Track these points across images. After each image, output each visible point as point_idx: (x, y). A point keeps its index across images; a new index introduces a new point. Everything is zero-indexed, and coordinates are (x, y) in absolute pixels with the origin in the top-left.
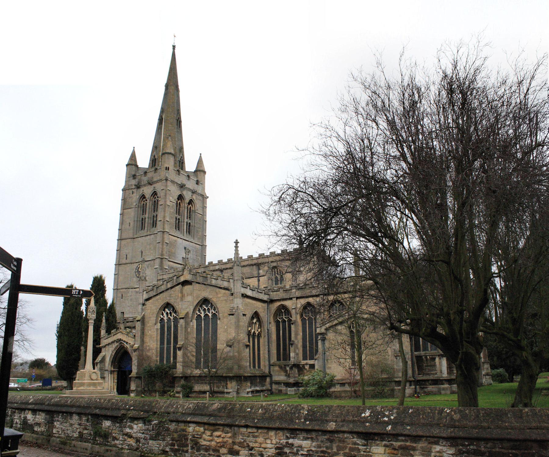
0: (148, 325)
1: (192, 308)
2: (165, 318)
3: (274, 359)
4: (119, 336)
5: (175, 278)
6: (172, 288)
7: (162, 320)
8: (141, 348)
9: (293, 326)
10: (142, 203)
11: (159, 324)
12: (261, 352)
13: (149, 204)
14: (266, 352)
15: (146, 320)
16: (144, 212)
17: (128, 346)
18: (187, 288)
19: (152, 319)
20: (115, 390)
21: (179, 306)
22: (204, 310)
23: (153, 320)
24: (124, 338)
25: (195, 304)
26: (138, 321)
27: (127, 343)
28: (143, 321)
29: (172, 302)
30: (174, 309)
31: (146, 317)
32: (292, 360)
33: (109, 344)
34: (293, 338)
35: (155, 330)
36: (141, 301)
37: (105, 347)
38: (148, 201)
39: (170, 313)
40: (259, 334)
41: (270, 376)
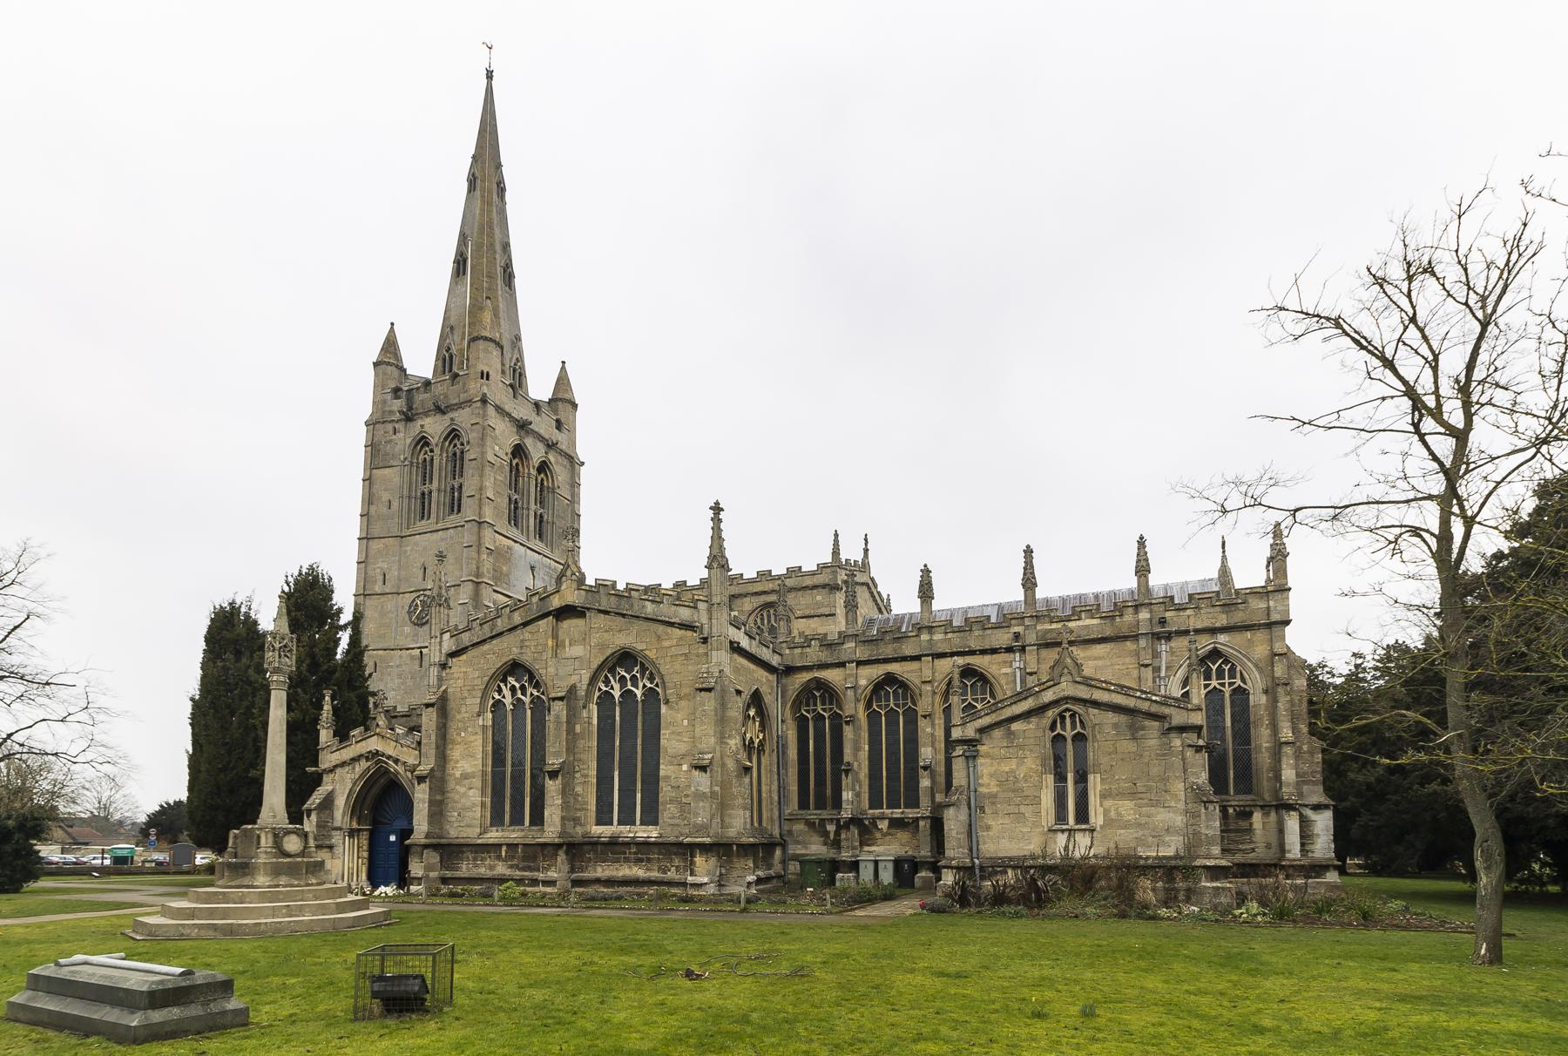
0: (458, 717)
1: (585, 681)
2: (508, 700)
3: (793, 805)
4: (373, 744)
5: (535, 599)
6: (525, 624)
7: (498, 705)
8: (438, 774)
9: (848, 731)
10: (421, 457)
11: (490, 715)
12: (764, 788)
13: (439, 460)
14: (775, 787)
15: (452, 705)
16: (426, 477)
17: (400, 769)
18: (571, 626)
19: (468, 701)
20: (364, 876)
21: (548, 670)
22: (622, 680)
23: (474, 702)
24: (389, 749)
25: (595, 665)
26: (427, 706)
27: (396, 761)
28: (442, 706)
29: (527, 658)
30: (532, 677)
31: (451, 697)
32: (846, 814)
33: (343, 764)
34: (848, 757)
35: (480, 731)
36: (436, 658)
37: (332, 770)
38: (437, 451)
39: (523, 688)
40: (761, 743)
41: (784, 845)
